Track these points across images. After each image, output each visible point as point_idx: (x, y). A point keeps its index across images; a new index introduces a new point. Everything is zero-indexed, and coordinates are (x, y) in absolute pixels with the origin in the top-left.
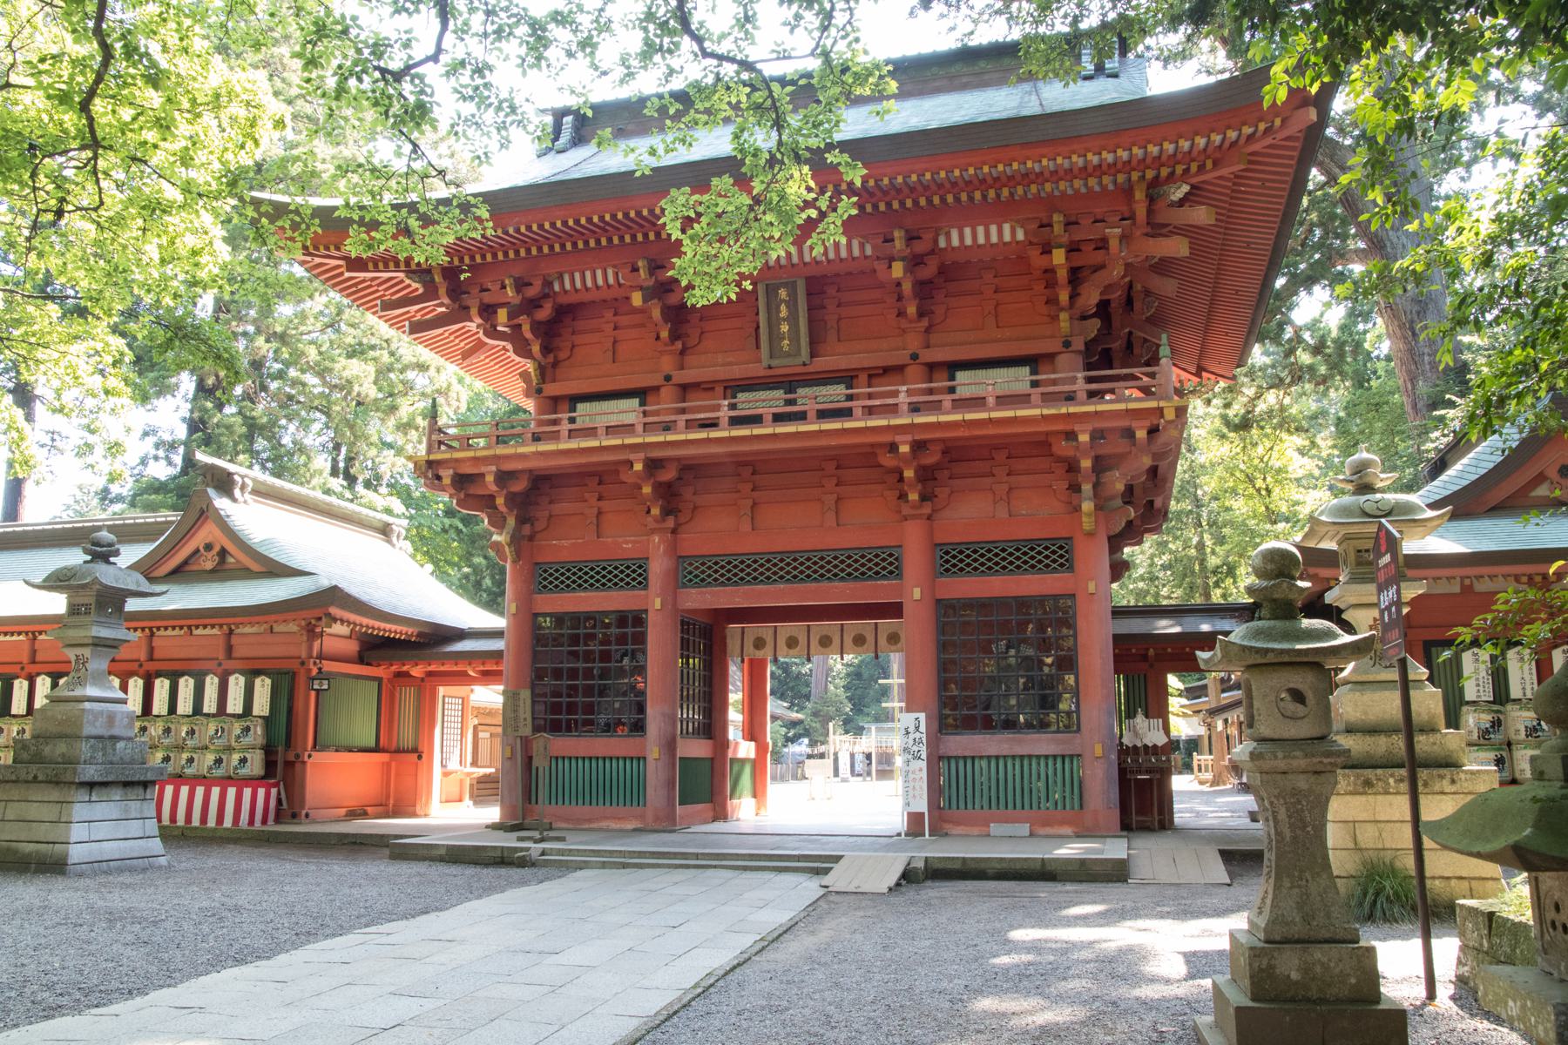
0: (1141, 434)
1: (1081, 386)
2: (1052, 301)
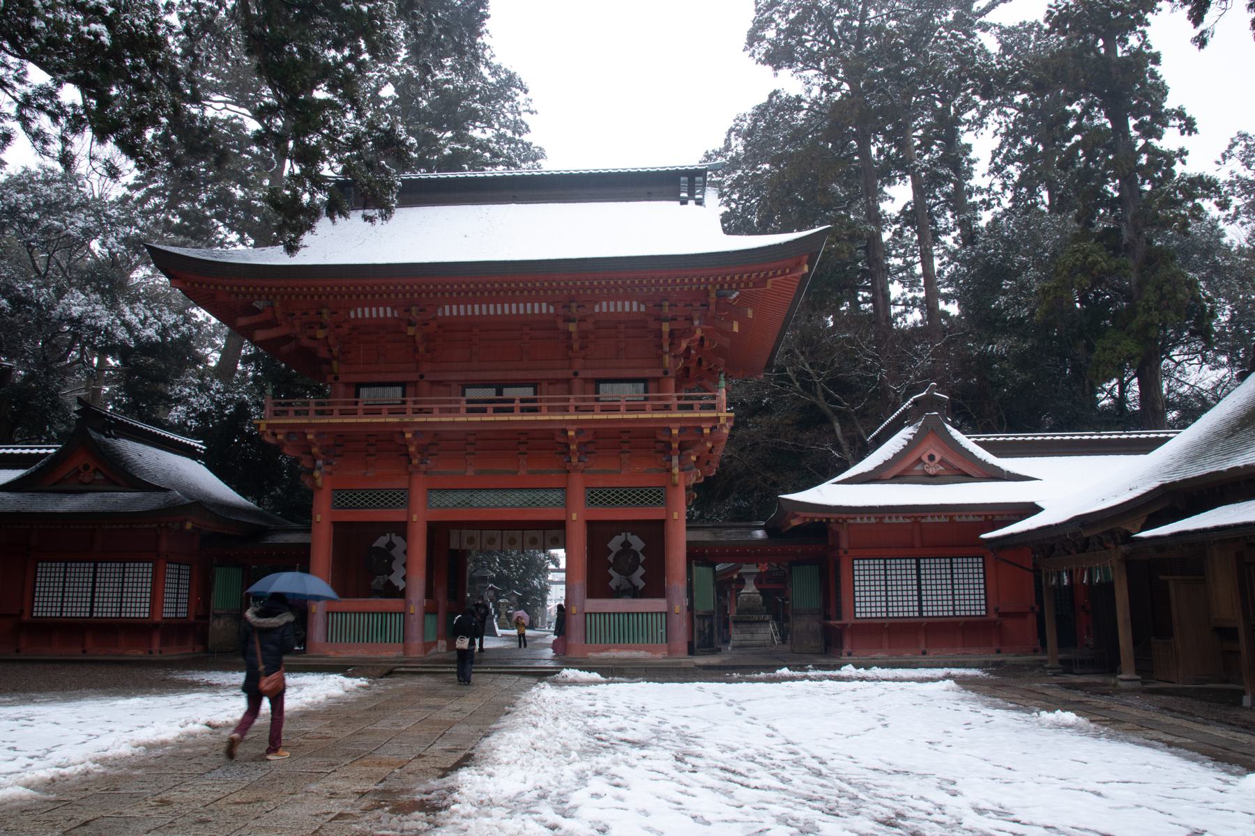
0: (707, 431)
1: (674, 402)
2: (661, 347)
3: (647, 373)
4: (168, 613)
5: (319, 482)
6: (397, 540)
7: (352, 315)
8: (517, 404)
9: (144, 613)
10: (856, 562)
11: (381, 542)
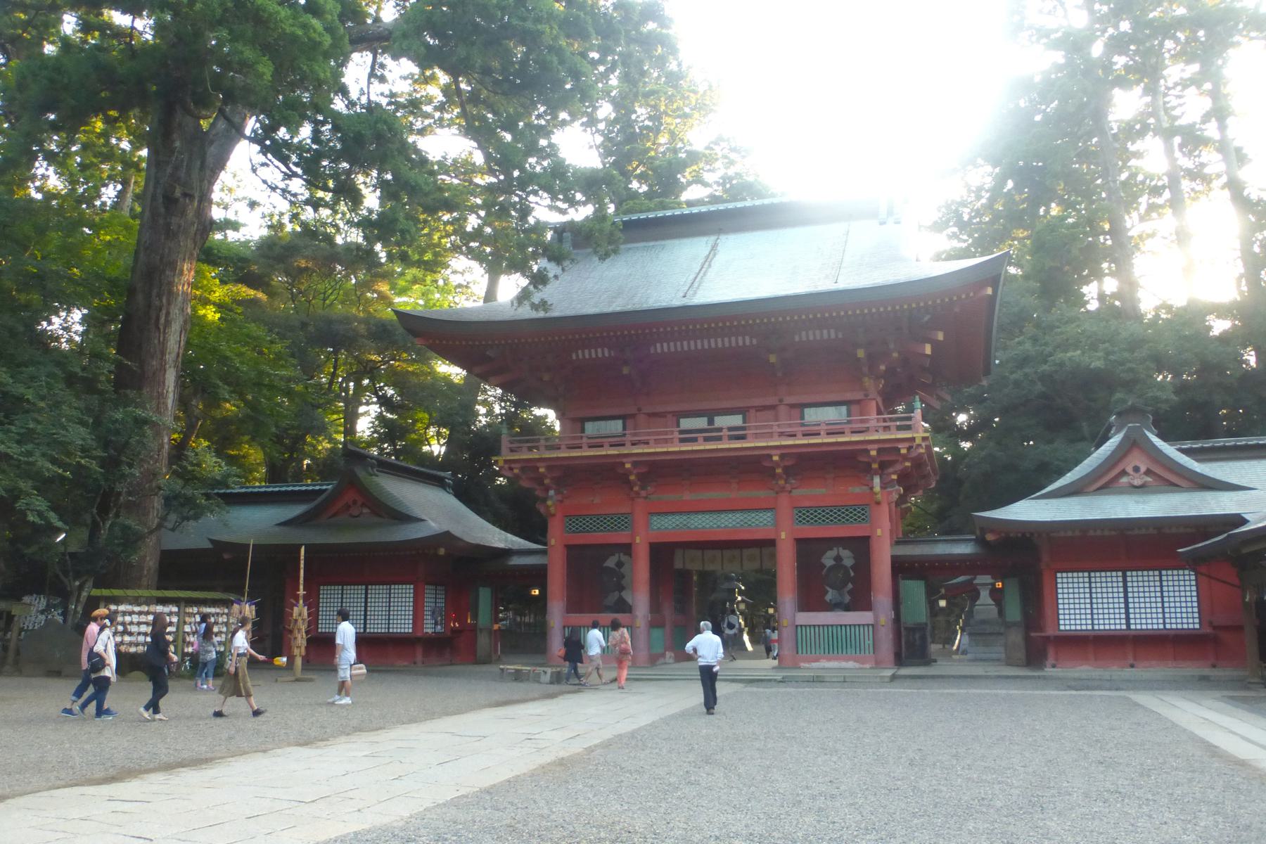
0: (904, 451)
3: (849, 396)
4: (429, 628)
5: (552, 510)
6: (624, 558)
7: (574, 357)
8: (725, 433)
9: (408, 629)
10: (1059, 575)
11: (611, 563)
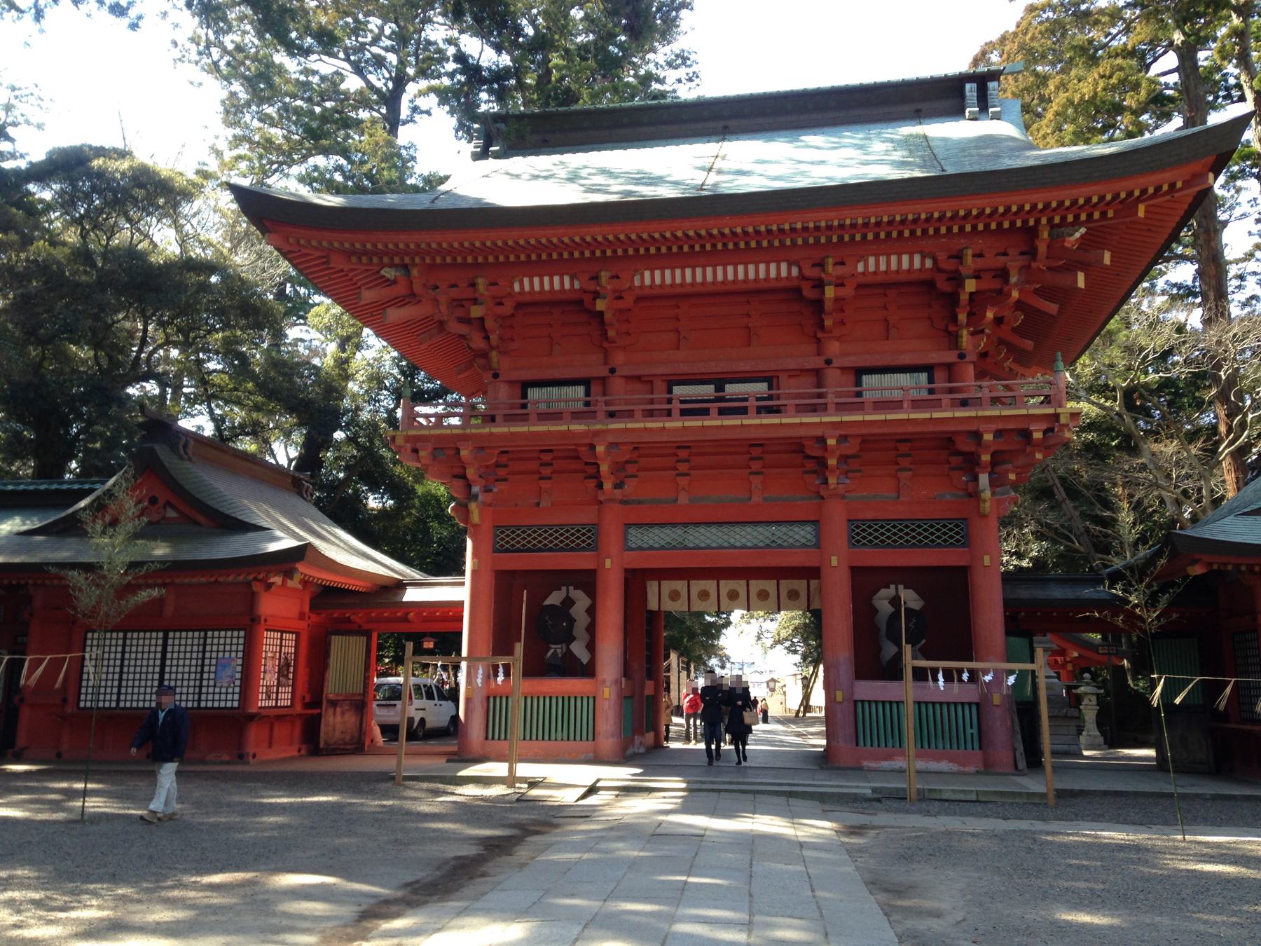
0: (1038, 435)
3: (934, 357)
7: (517, 287)
8: (752, 403)
